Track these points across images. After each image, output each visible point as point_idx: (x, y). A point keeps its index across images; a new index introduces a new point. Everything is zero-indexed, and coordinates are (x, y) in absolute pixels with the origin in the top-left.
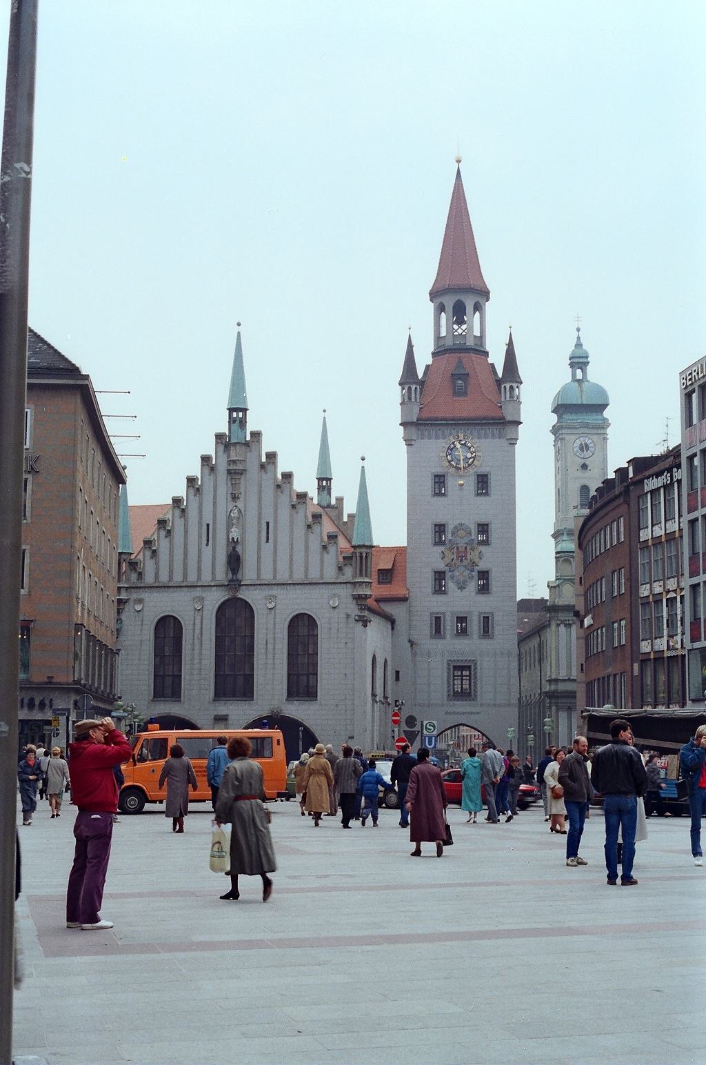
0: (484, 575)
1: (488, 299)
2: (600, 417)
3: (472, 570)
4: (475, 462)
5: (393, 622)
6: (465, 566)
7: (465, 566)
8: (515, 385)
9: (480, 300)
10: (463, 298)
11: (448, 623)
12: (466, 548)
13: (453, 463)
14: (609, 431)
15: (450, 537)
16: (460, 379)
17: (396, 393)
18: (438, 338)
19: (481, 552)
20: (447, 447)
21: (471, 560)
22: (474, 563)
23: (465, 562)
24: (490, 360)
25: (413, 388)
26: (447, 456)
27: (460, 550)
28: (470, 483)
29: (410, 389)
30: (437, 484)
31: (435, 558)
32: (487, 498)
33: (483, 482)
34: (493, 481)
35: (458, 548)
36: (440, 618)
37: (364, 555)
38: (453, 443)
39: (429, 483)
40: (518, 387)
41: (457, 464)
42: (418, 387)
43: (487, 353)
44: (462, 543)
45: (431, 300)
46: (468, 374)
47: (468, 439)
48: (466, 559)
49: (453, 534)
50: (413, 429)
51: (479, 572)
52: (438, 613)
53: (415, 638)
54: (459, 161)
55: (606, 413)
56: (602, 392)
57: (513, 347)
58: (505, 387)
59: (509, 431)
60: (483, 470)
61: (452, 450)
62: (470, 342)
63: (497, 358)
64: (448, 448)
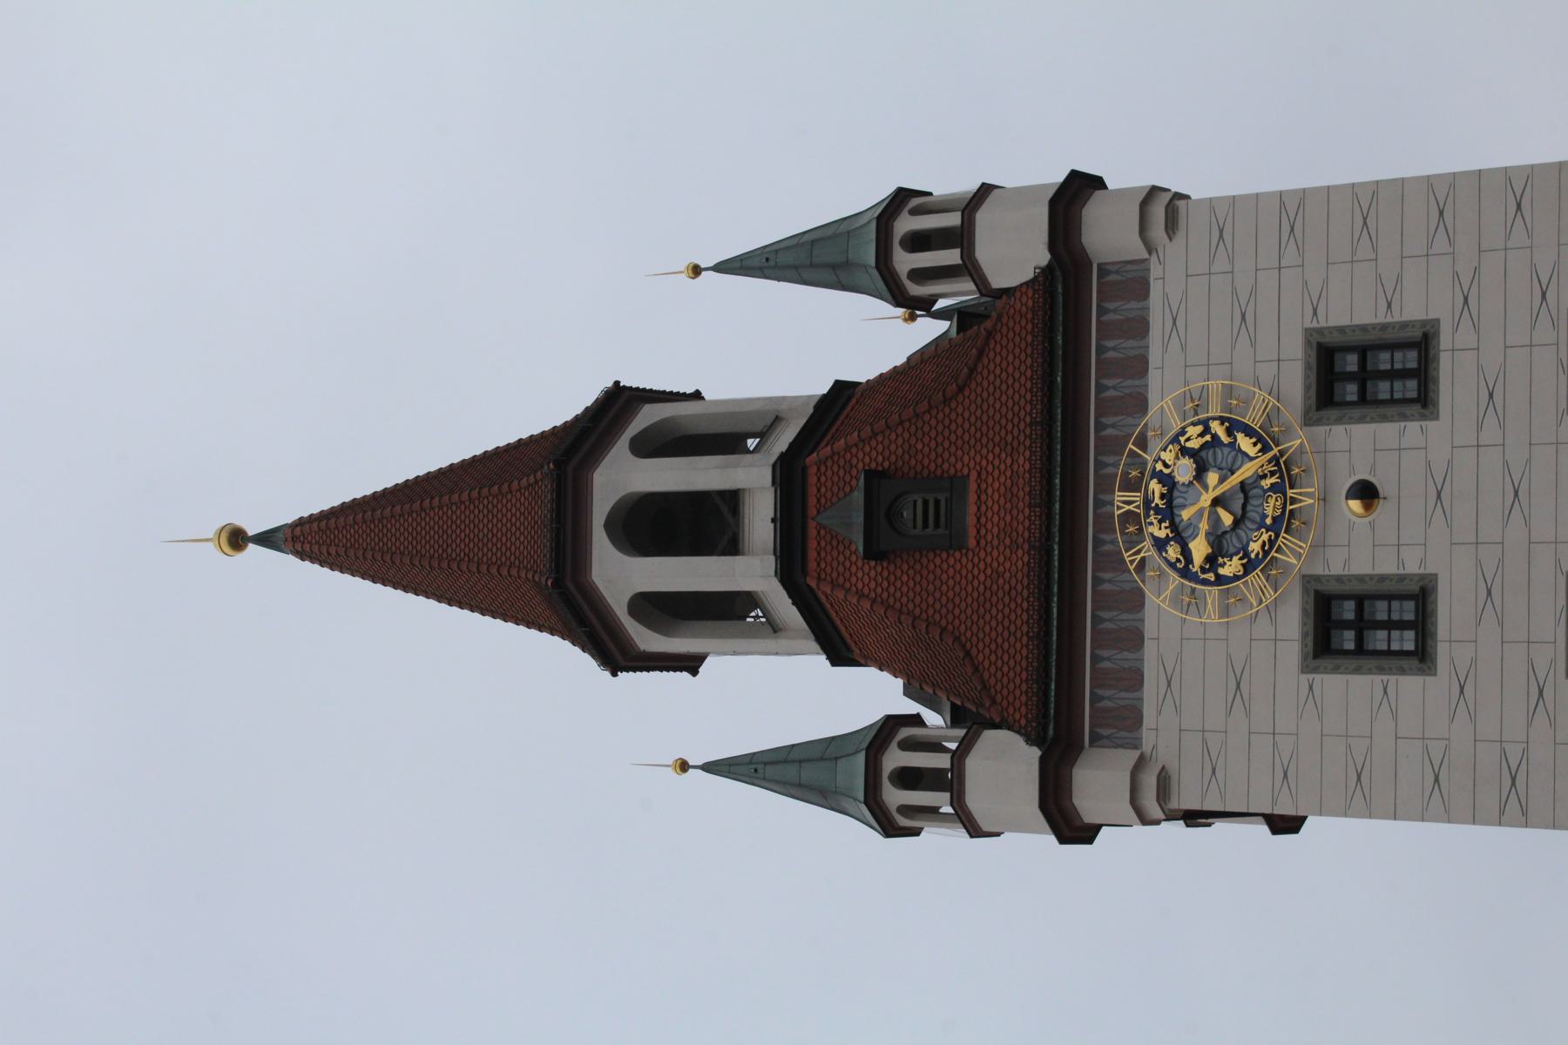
4: (1253, 418)
13: (1255, 547)
17: (940, 843)
20: (1174, 579)
25: (895, 758)
26: (1220, 580)
28: (1356, 445)
29: (909, 778)
30: (1378, 639)
32: (1445, 340)
33: (1370, 372)
34: (1354, 307)
38: (1160, 545)
39: (1350, 691)
41: (1262, 525)
43: (842, 390)
45: (691, 664)
47: (1145, 463)
54: (237, 539)
58: (919, 275)
59: (1107, 234)
60: (1295, 381)
64: (1185, 573)
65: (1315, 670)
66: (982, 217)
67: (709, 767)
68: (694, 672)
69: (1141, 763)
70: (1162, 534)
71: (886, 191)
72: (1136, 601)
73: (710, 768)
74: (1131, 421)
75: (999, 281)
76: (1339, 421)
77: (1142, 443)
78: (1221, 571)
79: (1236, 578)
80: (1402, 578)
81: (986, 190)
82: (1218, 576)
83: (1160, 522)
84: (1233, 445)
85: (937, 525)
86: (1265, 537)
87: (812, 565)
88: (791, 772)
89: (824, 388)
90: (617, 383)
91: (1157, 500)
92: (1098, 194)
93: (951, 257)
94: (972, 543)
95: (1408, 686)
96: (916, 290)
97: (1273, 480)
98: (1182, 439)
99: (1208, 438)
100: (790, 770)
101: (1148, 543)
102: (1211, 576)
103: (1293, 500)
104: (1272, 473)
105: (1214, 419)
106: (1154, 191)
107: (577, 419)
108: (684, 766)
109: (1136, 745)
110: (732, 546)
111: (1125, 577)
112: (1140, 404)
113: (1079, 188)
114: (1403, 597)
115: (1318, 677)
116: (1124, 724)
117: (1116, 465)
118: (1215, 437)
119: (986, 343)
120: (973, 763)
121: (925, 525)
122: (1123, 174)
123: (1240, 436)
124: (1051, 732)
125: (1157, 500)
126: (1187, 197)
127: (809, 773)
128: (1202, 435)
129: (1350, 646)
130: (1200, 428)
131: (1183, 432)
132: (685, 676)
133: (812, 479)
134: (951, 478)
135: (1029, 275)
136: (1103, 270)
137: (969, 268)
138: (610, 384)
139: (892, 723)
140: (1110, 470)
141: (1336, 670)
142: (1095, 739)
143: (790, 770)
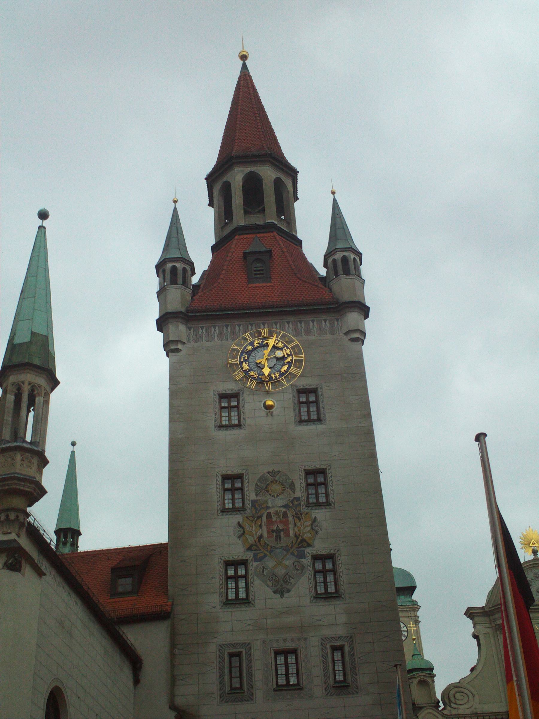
0: (326, 563)
2: (408, 600)
3: (302, 555)
5: (135, 662)
6: (287, 549)
7: (287, 549)
11: (258, 666)
12: (285, 515)
14: (419, 613)
15: (253, 497)
16: (259, 260)
17: (154, 283)
19: (315, 520)
21: (296, 537)
22: (303, 540)
23: (285, 542)
27: (274, 519)
31: (224, 537)
35: (269, 516)
36: (238, 655)
37: (26, 389)
43: (300, 242)
44: (276, 503)
46: (270, 252)
48: (288, 535)
49: (259, 490)
51: (316, 558)
52: (234, 645)
53: (179, 701)
55: (415, 597)
56: (407, 575)
57: (338, 206)
61: (249, 353)
63: (315, 249)
64: (243, 352)
67: (175, 210)
68: (209, 205)
70: (256, 344)
71: (361, 250)
73: (175, 210)
74: (291, 331)
76: (294, 396)
78: (244, 363)
79: (242, 368)
82: (242, 362)
83: (259, 343)
84: (284, 364)
85: (256, 274)
86: (255, 376)
87: (242, 237)
88: (174, 234)
90: (298, 172)
91: (266, 342)
92: (363, 317)
94: (250, 286)
97: (274, 377)
98: (285, 348)
99: (286, 356)
100: (175, 235)
101: (252, 340)
102: (242, 360)
103: (267, 384)
104: (276, 377)
105: (292, 357)
106: (364, 334)
107: (286, 161)
108: (175, 202)
110: (246, 212)
111: (241, 333)
113: (365, 311)
114: (239, 420)
117: (276, 328)
118: (287, 358)
119: (314, 285)
121: (255, 271)
122: (369, 325)
123: (287, 366)
124: (190, 314)
125: (266, 342)
126: (363, 344)
127: (174, 240)
128: (287, 354)
129: (223, 405)
130: (289, 353)
131: (288, 348)
132: (208, 202)
133: (269, 234)
134: (270, 278)
138: (298, 170)
139: (192, 265)
140: (274, 326)
143: (175, 235)
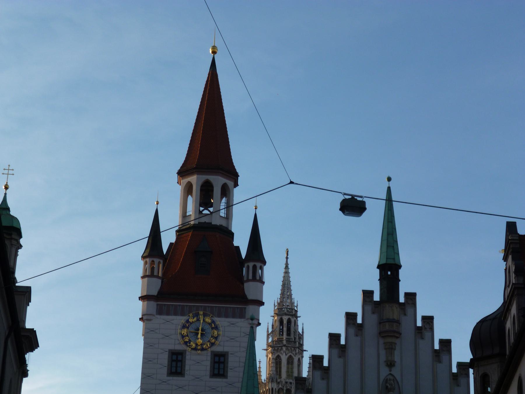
1: (236, 185)
8: (258, 265)
9: (230, 183)
10: (212, 178)
18: (184, 215)
24: (236, 243)
39: (164, 359)
40: (261, 268)
42: (162, 261)
43: (232, 234)
50: (153, 304)
62: (216, 221)
63: (241, 241)
65: (169, 352)
66: (259, 284)
69: (154, 315)
72: (183, 314)
75: (246, 285)
77: (212, 317)
80: (184, 370)
81: (263, 283)
89: (233, 231)
93: (250, 277)
95: (165, 371)
96: (246, 265)
109: (157, 314)
112: (219, 316)
115: (167, 353)
116: (160, 311)
120: (154, 280)
135: (246, 293)
136: (245, 308)
137: (248, 280)
141: (169, 356)
142: (157, 305)
